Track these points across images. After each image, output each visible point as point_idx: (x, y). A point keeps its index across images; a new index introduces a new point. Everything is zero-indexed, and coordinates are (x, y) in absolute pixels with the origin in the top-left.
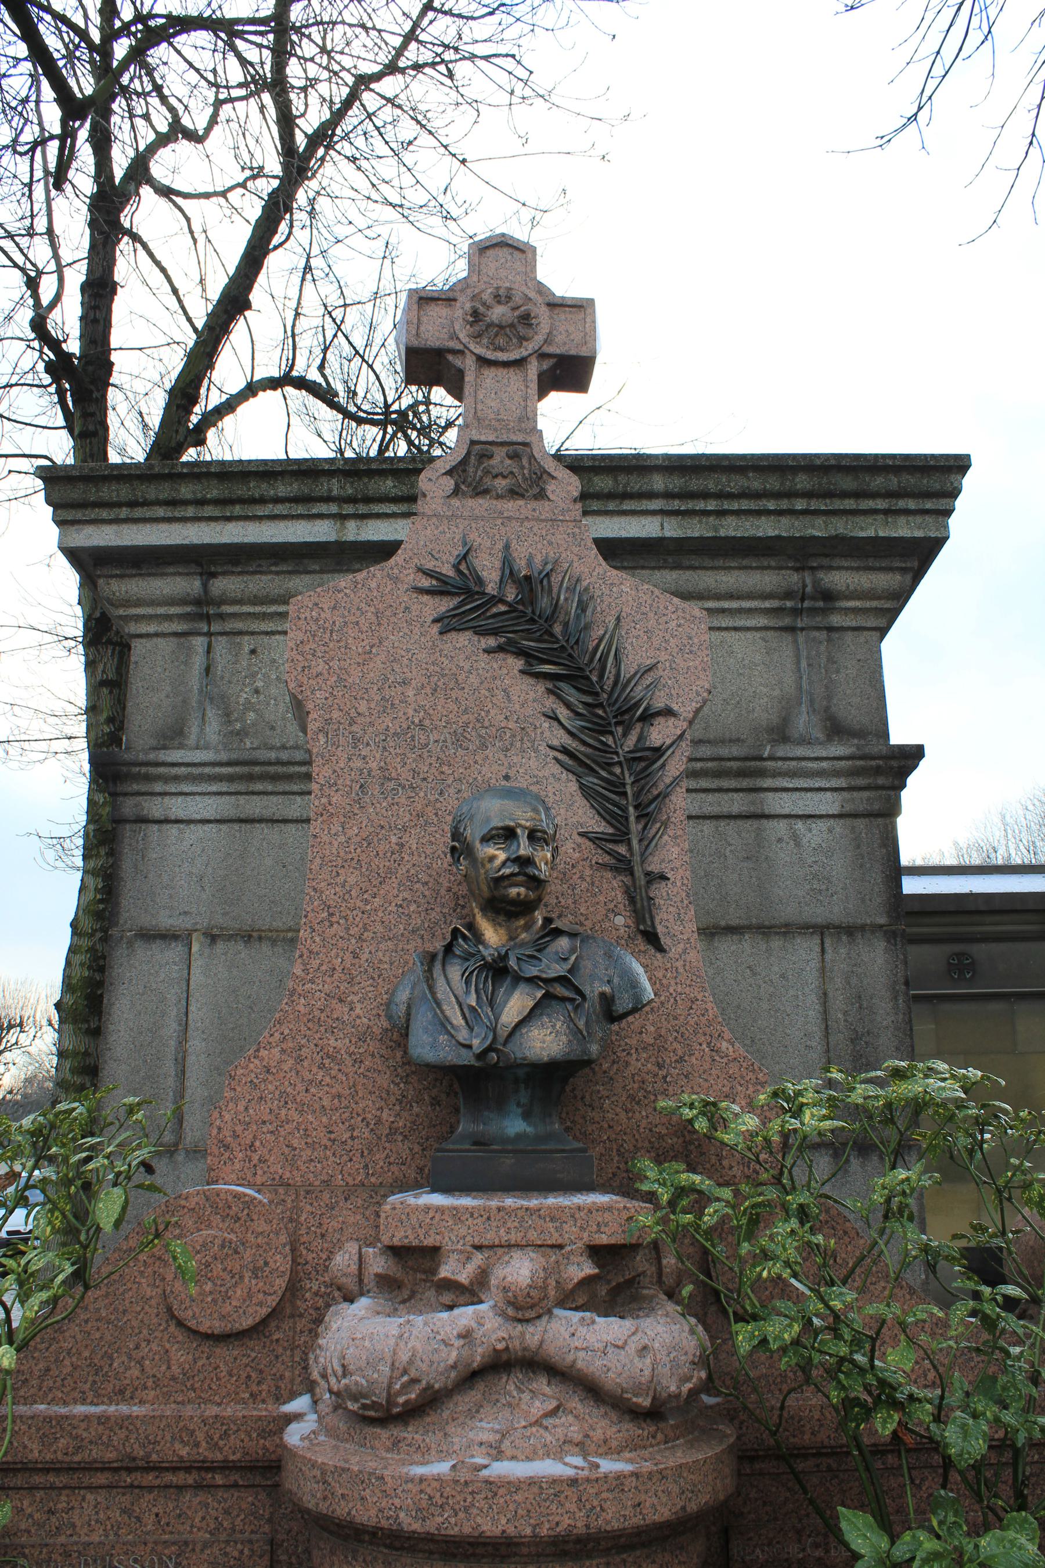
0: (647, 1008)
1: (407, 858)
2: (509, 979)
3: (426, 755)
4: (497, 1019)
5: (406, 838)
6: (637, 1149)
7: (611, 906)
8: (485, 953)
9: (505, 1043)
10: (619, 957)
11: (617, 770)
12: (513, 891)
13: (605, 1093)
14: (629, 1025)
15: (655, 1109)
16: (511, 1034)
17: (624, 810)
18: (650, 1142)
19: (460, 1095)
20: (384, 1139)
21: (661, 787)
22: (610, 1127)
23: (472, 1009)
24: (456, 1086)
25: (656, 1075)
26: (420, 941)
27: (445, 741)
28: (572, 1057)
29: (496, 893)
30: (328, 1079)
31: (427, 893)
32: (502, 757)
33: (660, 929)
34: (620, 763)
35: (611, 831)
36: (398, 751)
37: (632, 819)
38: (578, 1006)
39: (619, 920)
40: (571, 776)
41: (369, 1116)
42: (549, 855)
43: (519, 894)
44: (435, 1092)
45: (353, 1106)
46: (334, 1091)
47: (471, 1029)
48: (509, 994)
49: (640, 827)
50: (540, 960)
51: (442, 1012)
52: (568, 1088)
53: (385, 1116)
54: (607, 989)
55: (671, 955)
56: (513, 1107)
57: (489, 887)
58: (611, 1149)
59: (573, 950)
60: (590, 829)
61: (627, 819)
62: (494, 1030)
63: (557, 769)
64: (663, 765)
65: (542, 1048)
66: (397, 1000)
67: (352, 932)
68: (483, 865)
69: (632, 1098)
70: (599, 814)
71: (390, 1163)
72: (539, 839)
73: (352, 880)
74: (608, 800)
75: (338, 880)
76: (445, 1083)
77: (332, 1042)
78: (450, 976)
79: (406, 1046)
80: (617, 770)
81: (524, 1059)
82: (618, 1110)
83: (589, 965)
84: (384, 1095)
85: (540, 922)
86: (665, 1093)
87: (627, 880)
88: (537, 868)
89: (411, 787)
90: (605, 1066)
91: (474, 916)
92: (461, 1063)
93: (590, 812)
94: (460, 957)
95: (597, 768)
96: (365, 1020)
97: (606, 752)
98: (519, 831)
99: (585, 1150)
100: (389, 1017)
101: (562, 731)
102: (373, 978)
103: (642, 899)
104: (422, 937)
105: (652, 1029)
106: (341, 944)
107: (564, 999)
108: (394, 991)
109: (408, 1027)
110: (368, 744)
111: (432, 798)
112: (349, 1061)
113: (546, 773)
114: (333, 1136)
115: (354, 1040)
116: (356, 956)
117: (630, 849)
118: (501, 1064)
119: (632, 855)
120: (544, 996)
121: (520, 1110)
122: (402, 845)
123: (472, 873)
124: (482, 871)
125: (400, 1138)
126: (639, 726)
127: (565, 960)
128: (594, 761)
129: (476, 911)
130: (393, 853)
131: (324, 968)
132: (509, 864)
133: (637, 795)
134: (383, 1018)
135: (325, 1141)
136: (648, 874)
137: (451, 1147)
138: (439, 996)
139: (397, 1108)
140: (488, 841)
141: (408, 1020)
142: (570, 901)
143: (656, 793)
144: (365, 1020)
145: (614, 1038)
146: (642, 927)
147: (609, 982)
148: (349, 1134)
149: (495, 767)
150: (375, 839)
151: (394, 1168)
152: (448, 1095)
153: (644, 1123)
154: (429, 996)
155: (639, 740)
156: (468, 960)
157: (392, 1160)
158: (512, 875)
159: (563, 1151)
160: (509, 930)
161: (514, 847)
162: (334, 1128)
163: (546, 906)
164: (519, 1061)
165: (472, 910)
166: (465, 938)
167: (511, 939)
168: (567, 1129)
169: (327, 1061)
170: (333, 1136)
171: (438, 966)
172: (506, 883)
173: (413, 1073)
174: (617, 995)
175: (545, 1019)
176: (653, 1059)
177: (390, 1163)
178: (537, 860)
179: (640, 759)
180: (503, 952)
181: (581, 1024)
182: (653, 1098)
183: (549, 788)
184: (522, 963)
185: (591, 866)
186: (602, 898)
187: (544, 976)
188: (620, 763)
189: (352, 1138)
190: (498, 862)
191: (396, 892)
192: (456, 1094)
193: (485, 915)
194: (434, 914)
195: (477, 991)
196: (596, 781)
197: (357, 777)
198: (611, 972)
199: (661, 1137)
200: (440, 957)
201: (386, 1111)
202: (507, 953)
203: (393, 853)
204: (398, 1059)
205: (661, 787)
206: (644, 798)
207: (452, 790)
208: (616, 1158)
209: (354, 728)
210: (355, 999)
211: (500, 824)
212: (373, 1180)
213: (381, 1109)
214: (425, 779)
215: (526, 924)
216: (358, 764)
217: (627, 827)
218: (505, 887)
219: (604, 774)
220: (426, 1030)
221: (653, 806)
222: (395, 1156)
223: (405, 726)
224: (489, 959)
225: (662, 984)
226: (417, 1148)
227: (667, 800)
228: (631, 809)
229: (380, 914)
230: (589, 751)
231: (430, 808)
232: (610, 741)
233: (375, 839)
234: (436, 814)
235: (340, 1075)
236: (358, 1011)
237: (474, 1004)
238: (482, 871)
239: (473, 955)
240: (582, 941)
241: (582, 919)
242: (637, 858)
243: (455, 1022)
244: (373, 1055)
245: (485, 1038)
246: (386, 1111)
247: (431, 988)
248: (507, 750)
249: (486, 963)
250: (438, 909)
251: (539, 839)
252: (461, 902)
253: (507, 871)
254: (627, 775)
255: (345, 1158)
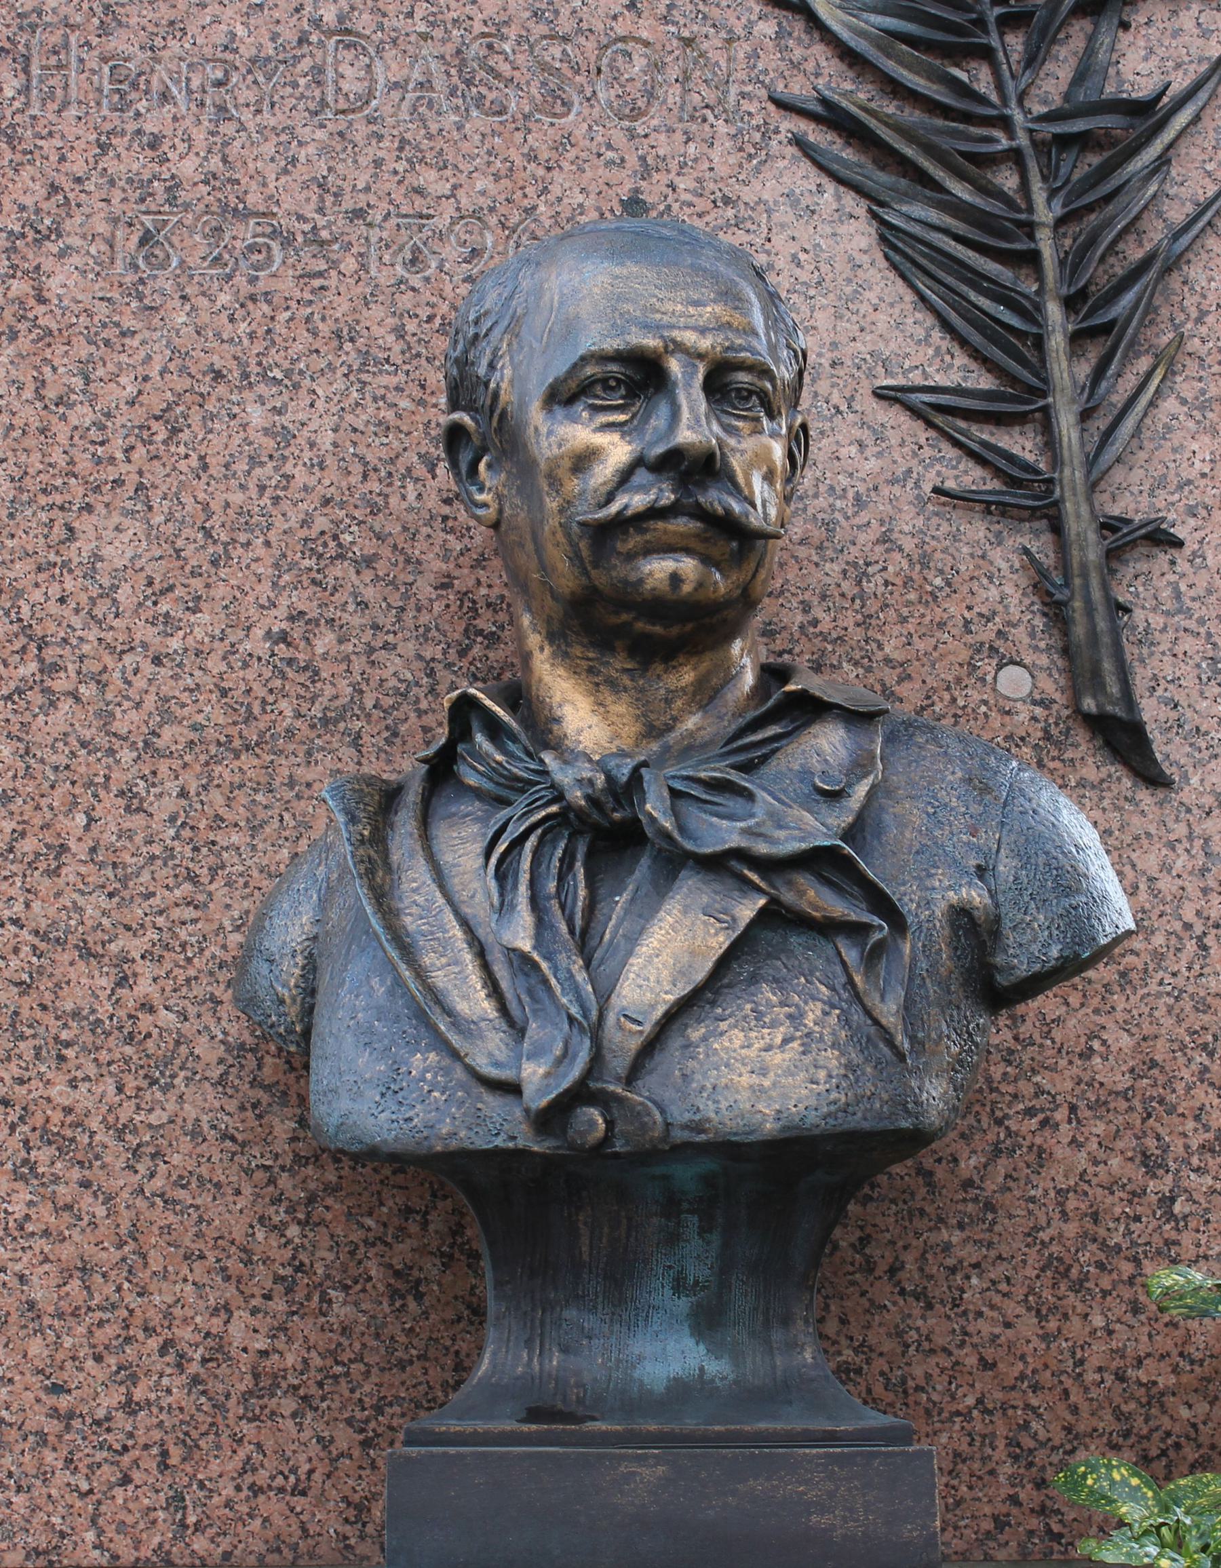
0: (1102, 973)
1: (301, 476)
2: (645, 862)
3: (361, 131)
4: (604, 997)
5: (297, 412)
6: (1075, 1438)
7: (987, 634)
8: (564, 776)
9: (632, 1076)
10: (1015, 790)
11: (1008, 180)
12: (658, 569)
13: (970, 1254)
14: (1048, 1025)
15: (1136, 1308)
16: (652, 1046)
17: (1031, 312)
18: (1118, 1414)
19: (486, 1263)
20: (235, 1408)
21: (1155, 234)
22: (986, 1365)
23: (522, 963)
24: (473, 1231)
25: (1137, 1195)
26: (347, 753)
27: (425, 85)
28: (857, 1121)
29: (600, 579)
30: (46, 1215)
31: (369, 593)
32: (619, 138)
33: (1151, 711)
34: (1015, 157)
35: (986, 382)
36: (267, 118)
37: (1057, 342)
38: (880, 947)
39: (1014, 682)
40: (850, 200)
41: (185, 1334)
42: (778, 451)
43: (675, 579)
44: (402, 1253)
45: (132, 1300)
46: (67, 1252)
47: (517, 1030)
48: (645, 911)
49: (1084, 370)
50: (749, 796)
51: (420, 974)
52: (844, 1236)
53: (237, 1332)
54: (976, 895)
55: (1187, 796)
56: (661, 1294)
57: (576, 557)
58: (988, 1438)
59: (859, 766)
60: (916, 379)
61: (1039, 343)
62: (596, 1032)
63: (803, 177)
64: (1163, 161)
65: (758, 1092)
66: (272, 944)
67: (121, 727)
68: (555, 482)
69: (1058, 1269)
70: (946, 326)
71: (256, 1490)
72: (745, 394)
73: (117, 553)
74: (976, 279)
75: (71, 552)
76: (437, 1223)
77: (59, 1091)
78: (447, 858)
79: (303, 1100)
80: (1008, 180)
81: (697, 1127)
82: (1012, 1308)
83: (917, 817)
84: (234, 1265)
85: (749, 679)
86: (1169, 1255)
87: (1041, 545)
88: (736, 490)
89: (314, 239)
90: (969, 1164)
91: (526, 657)
92: (482, 1143)
93: (919, 322)
94: (478, 793)
95: (938, 173)
96: (167, 1018)
97: (967, 118)
98: (675, 366)
99: (904, 1436)
100: (247, 1004)
101: (819, 52)
102: (193, 878)
103: (1090, 610)
104: (356, 741)
105: (1126, 1041)
106: (84, 764)
107: (828, 928)
108: (262, 916)
109: (307, 1034)
110: (165, 97)
111: (384, 278)
112: (116, 1156)
113: (767, 188)
114: (64, 1402)
115: (131, 1083)
116: (133, 804)
117: (1051, 444)
118: (619, 1147)
119: (1056, 461)
120: (762, 912)
121: (683, 1304)
122: (285, 436)
123: (517, 512)
124: (552, 504)
125: (289, 1405)
126: (1079, 30)
127: (834, 796)
128: (930, 150)
129: (534, 640)
130: (254, 461)
131: (28, 845)
132: (641, 476)
133: (1072, 263)
134: (225, 1010)
135: (38, 1419)
136: (1109, 526)
137: (455, 1426)
138: (410, 922)
139: (279, 1305)
140: (571, 400)
141: (310, 992)
142: (849, 619)
143: (1135, 253)
144: (167, 1018)
145: (997, 1072)
146: (1089, 704)
147: (981, 871)
148: (116, 1396)
149: (596, 173)
150: (196, 417)
151: (271, 1505)
152: (448, 1261)
153: (1097, 1353)
154: (376, 924)
155: (1080, 77)
156: (506, 802)
157: (262, 1477)
158: (654, 513)
159: (830, 1438)
160: (641, 699)
161: (659, 420)
162: (69, 1375)
163: (769, 633)
164: (679, 1136)
165: (520, 638)
166: (495, 729)
167: (652, 731)
168: (845, 1372)
169: (42, 1155)
170: (64, 1402)
171: (405, 823)
172: (634, 541)
173: (332, 1189)
174: (1010, 915)
175: (767, 994)
176: (1127, 1142)
177: (256, 1490)
178: (736, 463)
179: (1083, 141)
180: (624, 774)
181: (889, 1011)
182: (1127, 1268)
183: (778, 240)
184: (682, 804)
185: (921, 502)
186: (955, 609)
187: (762, 848)
188: (1015, 157)
189: (130, 1407)
190: (604, 472)
191: (265, 590)
192: (475, 1256)
193: (562, 656)
194: (393, 664)
195: (535, 903)
196: (933, 216)
197: (131, 209)
198: (987, 838)
199: (1155, 1398)
200: (413, 796)
201: (241, 1317)
202: (636, 776)
203: (254, 461)
204: (281, 1146)
205: (1155, 234)
206: (1099, 275)
207: (451, 252)
208: (1007, 1469)
209: (118, 43)
210: (135, 946)
211: (612, 344)
212: (200, 1544)
213: (226, 1309)
214: (358, 214)
215: (700, 684)
216: (134, 162)
217: (1040, 369)
218: (631, 557)
219: (961, 191)
220: (367, 1039)
221: (1128, 298)
222: (271, 1464)
223: (289, 34)
224: (577, 796)
225: (1155, 893)
226: (345, 1438)
227: (1175, 281)
228: (1054, 311)
229: (215, 665)
230: (912, 116)
231: (377, 312)
232: (982, 80)
233: (196, 417)
234: (400, 332)
235: (86, 1201)
236: (144, 987)
237: (526, 945)
238: (552, 504)
239: (520, 785)
240: (890, 739)
241: (890, 676)
242: (1073, 474)
243: (462, 1007)
244: (196, 1134)
245: (567, 1055)
246: (241, 1317)
247: (382, 897)
248: (636, 113)
249: (568, 809)
250: (409, 648)
251: (745, 394)
252: (485, 623)
253: (635, 501)
254: (1039, 195)
255: (108, 1473)
